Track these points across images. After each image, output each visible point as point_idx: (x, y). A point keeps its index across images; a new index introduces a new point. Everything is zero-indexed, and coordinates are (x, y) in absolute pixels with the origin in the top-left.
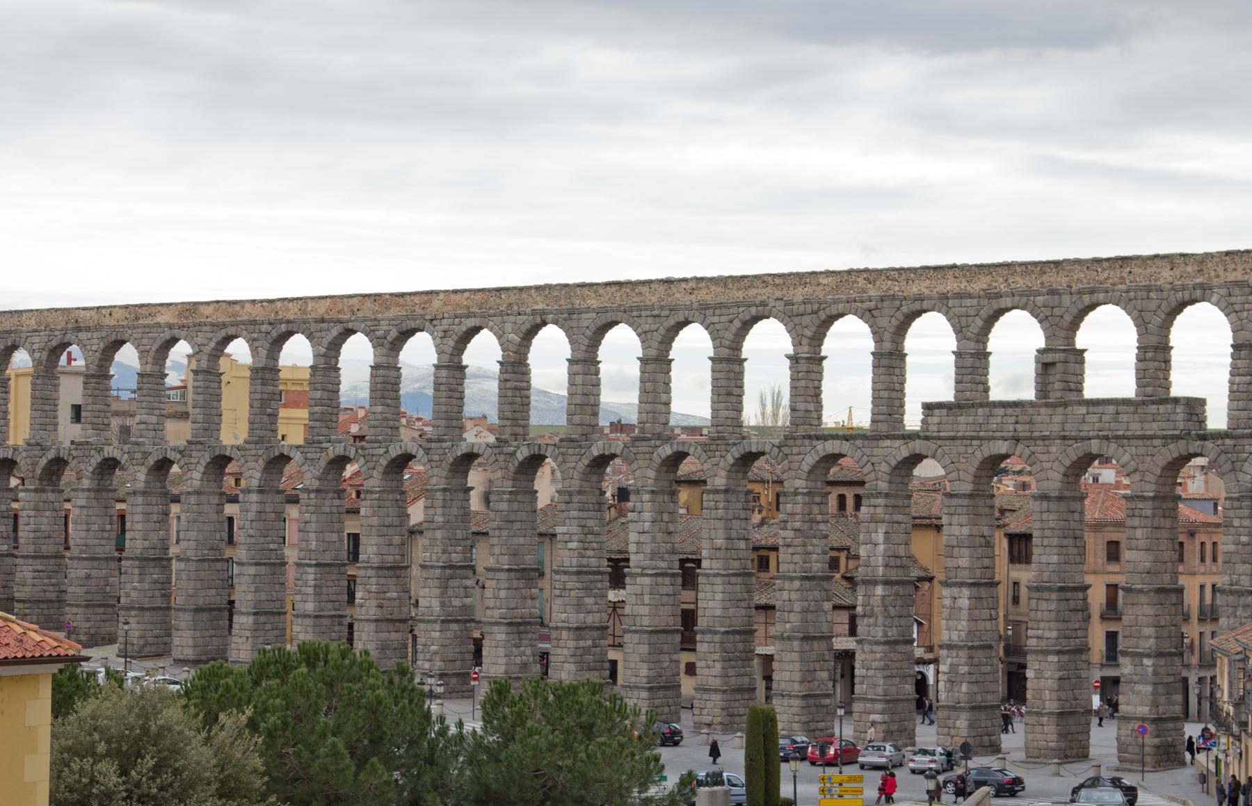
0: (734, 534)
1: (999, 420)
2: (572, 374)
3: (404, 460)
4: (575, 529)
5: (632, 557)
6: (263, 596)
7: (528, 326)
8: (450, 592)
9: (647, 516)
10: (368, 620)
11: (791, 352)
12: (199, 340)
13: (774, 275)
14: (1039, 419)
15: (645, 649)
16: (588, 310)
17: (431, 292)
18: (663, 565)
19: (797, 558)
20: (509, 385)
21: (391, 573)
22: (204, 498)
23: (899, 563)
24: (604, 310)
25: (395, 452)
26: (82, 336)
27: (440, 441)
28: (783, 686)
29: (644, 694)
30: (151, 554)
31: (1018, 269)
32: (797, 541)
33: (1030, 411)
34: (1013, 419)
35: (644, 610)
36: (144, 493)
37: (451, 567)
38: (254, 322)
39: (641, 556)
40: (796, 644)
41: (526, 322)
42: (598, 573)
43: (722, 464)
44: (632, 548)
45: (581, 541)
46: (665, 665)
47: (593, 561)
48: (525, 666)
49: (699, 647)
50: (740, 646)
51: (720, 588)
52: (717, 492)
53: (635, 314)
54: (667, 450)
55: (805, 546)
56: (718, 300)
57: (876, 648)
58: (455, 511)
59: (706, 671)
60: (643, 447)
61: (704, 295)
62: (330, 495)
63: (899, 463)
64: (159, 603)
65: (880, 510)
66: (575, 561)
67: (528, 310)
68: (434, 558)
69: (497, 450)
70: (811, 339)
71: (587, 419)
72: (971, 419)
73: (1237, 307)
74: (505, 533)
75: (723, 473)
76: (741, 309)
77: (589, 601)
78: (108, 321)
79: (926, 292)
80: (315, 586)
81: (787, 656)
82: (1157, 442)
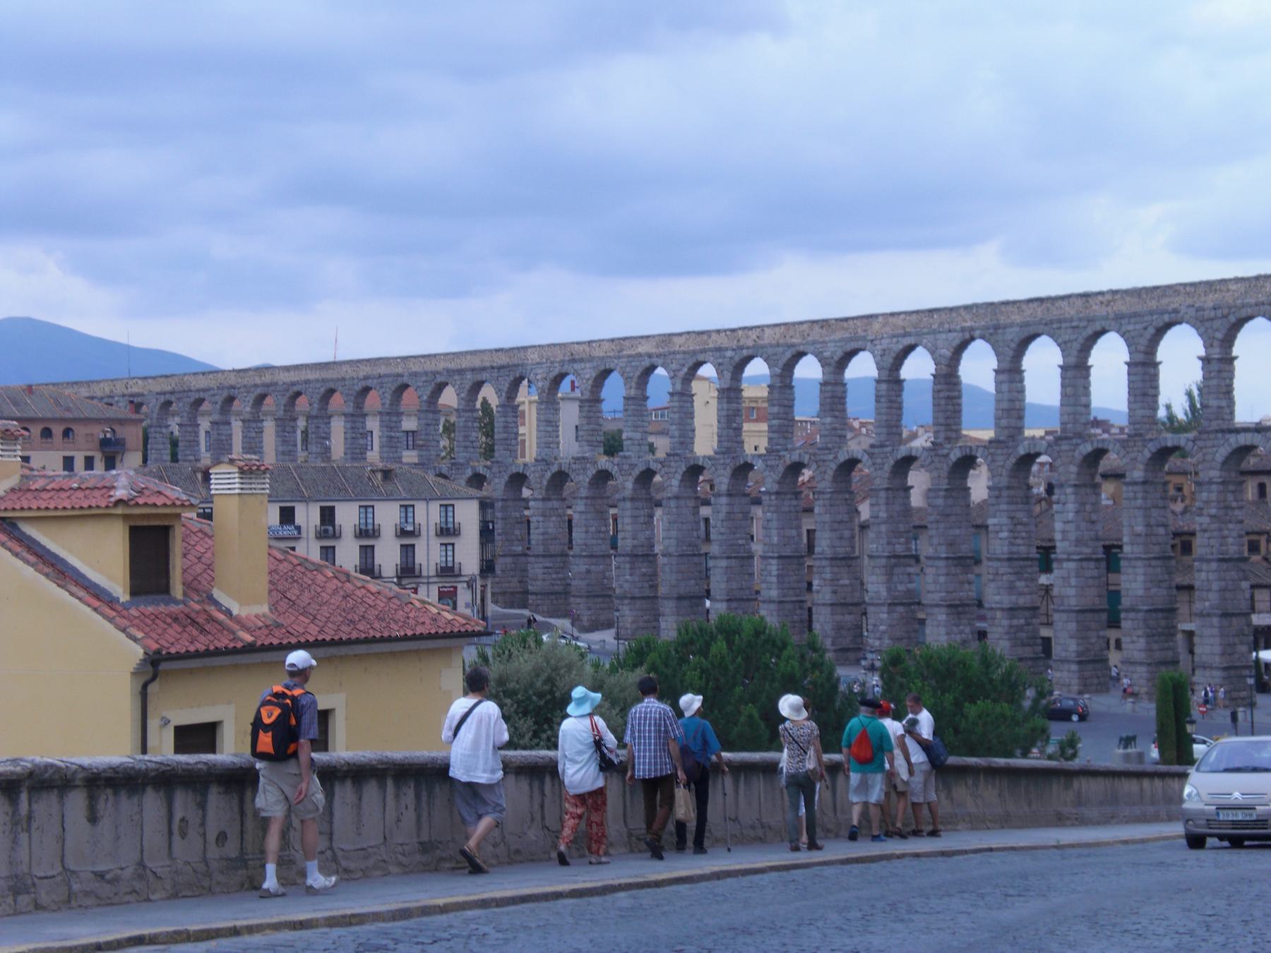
0: (1153, 521)
3: (852, 463)
4: (1005, 520)
5: (1058, 544)
6: (734, 585)
7: (957, 342)
8: (895, 578)
9: (1071, 507)
10: (824, 605)
11: (1202, 352)
12: (674, 366)
13: (1185, 285)
15: (1072, 626)
16: (1012, 325)
19: (1213, 542)
20: (942, 395)
22: (682, 502)
25: (842, 457)
26: (576, 366)
27: (882, 446)
28: (1204, 658)
29: (1074, 667)
30: (640, 551)
32: (1215, 526)
36: (633, 499)
37: (895, 557)
38: (719, 349)
39: (1066, 544)
40: (1215, 621)
41: (956, 338)
42: (1027, 559)
44: (1058, 536)
46: (1093, 640)
47: (1022, 548)
49: (1123, 624)
50: (1163, 623)
51: (1141, 571)
52: (1135, 483)
53: (1055, 326)
54: (1088, 448)
55: (1220, 530)
56: (1133, 309)
58: (897, 508)
59: (1131, 646)
60: (1065, 446)
61: (1121, 307)
62: (789, 496)
64: (647, 593)
66: (1006, 549)
67: (958, 328)
68: (880, 549)
70: (1222, 341)
74: (942, 526)
75: (1141, 467)
76: (1155, 317)
77: (1020, 584)
78: (598, 353)
80: (778, 576)
81: (1207, 632)
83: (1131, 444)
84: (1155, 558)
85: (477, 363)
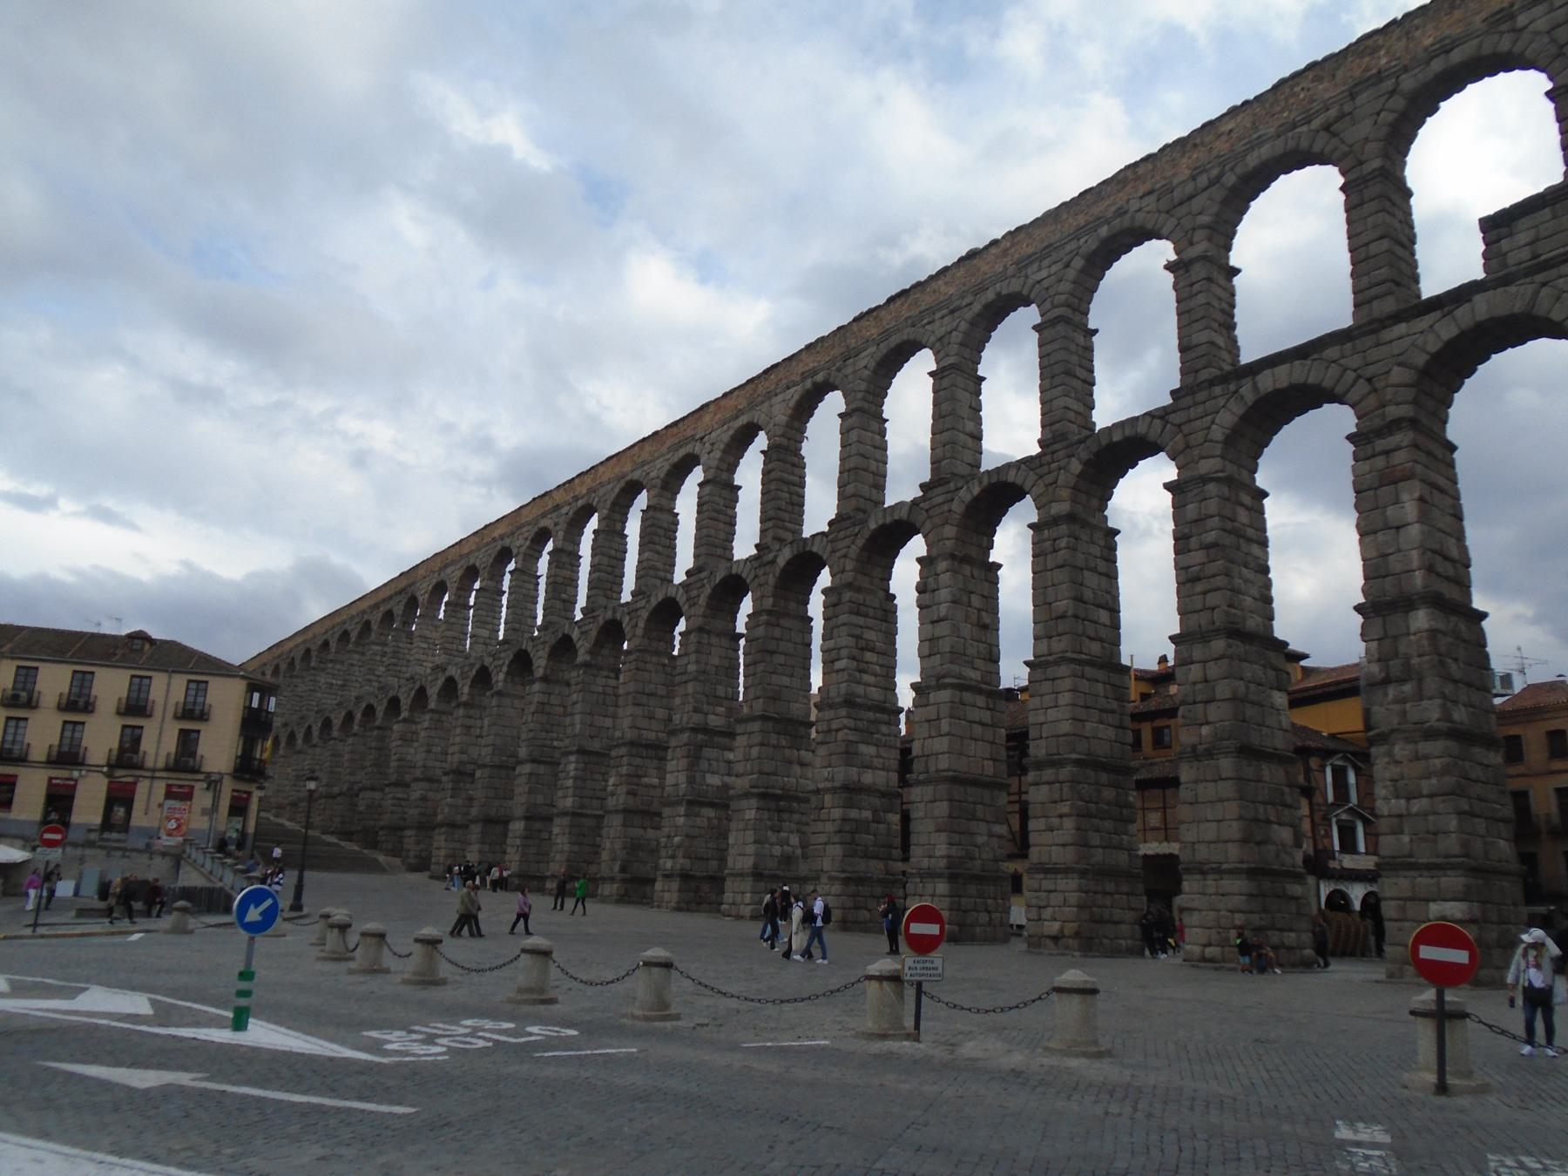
0: (1088, 595)
2: (844, 432)
8: (704, 765)
10: (616, 812)
15: (943, 808)
17: (703, 407)
18: (974, 675)
19: (1214, 599)
21: (651, 753)
23: (1451, 572)
24: (886, 334)
28: (1203, 853)
32: (1212, 568)
35: (941, 744)
38: (557, 507)
40: (1226, 764)
41: (794, 394)
45: (854, 658)
46: (980, 840)
48: (787, 860)
51: (1067, 684)
57: (1437, 746)
59: (1047, 837)
63: (1436, 358)
65: (1400, 457)
67: (798, 379)
69: (756, 564)
75: (1065, 493)
77: (867, 750)
79: (1456, 31)
80: (575, 778)
81: (1208, 791)
83: (1048, 458)
84: (1091, 663)
85: (388, 593)
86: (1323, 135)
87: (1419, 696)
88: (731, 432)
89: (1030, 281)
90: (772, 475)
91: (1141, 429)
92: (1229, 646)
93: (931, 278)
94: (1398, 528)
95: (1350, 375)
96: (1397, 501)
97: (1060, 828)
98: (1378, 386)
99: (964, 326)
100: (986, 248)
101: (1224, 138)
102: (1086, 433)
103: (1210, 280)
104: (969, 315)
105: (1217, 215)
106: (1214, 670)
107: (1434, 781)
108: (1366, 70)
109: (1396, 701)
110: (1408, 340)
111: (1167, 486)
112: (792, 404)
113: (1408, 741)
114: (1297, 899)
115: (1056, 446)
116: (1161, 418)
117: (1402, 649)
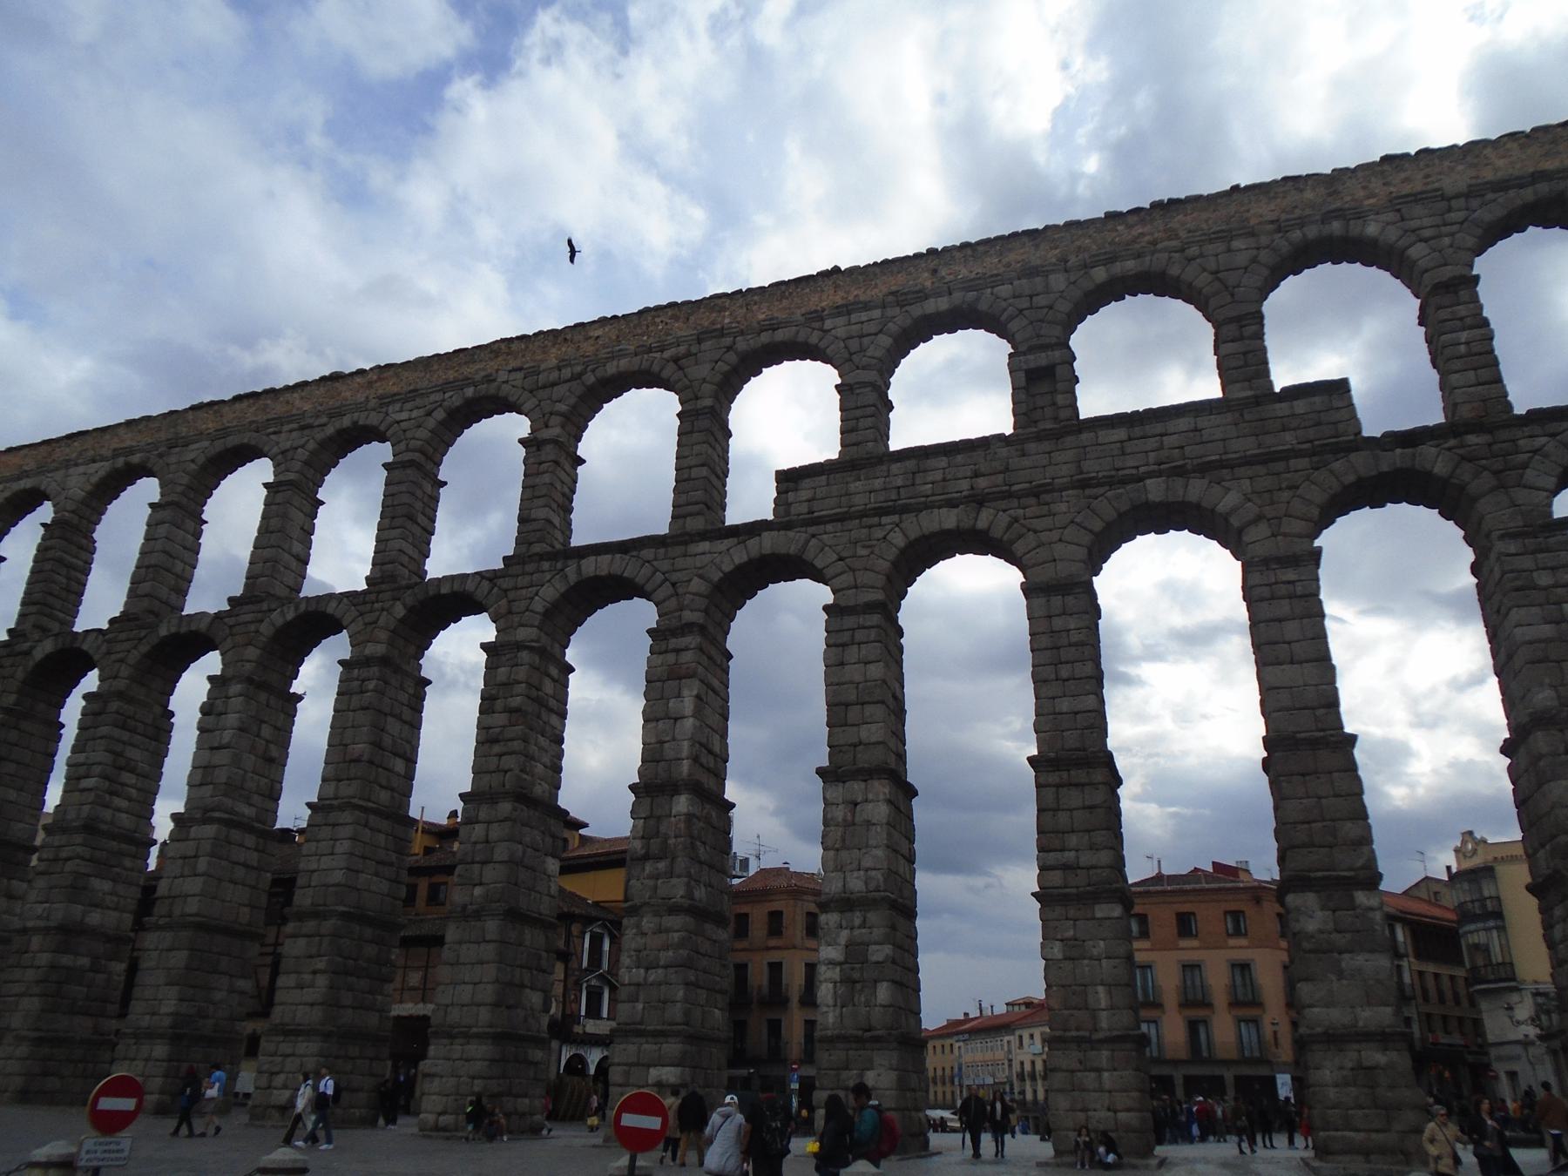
0: (387, 741)
1: (938, 476)
14: (1026, 462)
15: (179, 958)
18: (248, 811)
19: (509, 762)
24: (224, 432)
28: (455, 1015)
31: (958, 255)
32: (512, 732)
33: (1003, 452)
34: (968, 471)
35: (194, 885)
40: (492, 926)
41: (100, 469)
43: (381, 622)
45: (106, 777)
46: (218, 996)
50: (371, 950)
51: (347, 831)
61: (390, 387)
63: (727, 577)
65: (687, 657)
67: (109, 453)
71: (164, 592)
72: (878, 483)
73: (1427, 233)
75: (383, 635)
77: (101, 886)
79: (782, 316)
82: (1303, 463)
83: (373, 597)
84: (376, 812)
86: (671, 366)
87: (670, 874)
88: (7, 494)
89: (389, 420)
90: (50, 554)
91: (470, 586)
92: (515, 809)
93: (287, 388)
94: (676, 719)
95: (659, 577)
96: (679, 696)
97: (312, 986)
98: (680, 591)
99: (312, 445)
100: (352, 374)
101: (592, 341)
102: (415, 579)
103: (557, 463)
104: (319, 436)
105: (574, 407)
106: (496, 832)
107: (671, 953)
108: (713, 323)
109: (650, 877)
110: (707, 558)
111: (484, 646)
112: (94, 479)
113: (657, 914)
114: (536, 1063)
115: (383, 587)
116: (490, 580)
117: (663, 829)
